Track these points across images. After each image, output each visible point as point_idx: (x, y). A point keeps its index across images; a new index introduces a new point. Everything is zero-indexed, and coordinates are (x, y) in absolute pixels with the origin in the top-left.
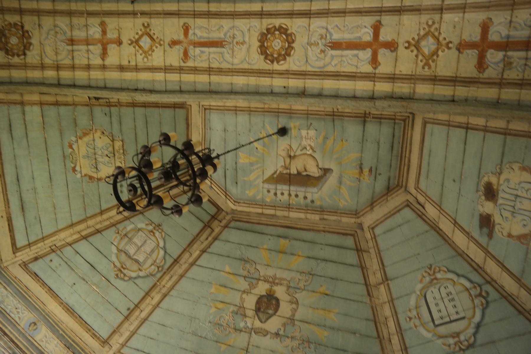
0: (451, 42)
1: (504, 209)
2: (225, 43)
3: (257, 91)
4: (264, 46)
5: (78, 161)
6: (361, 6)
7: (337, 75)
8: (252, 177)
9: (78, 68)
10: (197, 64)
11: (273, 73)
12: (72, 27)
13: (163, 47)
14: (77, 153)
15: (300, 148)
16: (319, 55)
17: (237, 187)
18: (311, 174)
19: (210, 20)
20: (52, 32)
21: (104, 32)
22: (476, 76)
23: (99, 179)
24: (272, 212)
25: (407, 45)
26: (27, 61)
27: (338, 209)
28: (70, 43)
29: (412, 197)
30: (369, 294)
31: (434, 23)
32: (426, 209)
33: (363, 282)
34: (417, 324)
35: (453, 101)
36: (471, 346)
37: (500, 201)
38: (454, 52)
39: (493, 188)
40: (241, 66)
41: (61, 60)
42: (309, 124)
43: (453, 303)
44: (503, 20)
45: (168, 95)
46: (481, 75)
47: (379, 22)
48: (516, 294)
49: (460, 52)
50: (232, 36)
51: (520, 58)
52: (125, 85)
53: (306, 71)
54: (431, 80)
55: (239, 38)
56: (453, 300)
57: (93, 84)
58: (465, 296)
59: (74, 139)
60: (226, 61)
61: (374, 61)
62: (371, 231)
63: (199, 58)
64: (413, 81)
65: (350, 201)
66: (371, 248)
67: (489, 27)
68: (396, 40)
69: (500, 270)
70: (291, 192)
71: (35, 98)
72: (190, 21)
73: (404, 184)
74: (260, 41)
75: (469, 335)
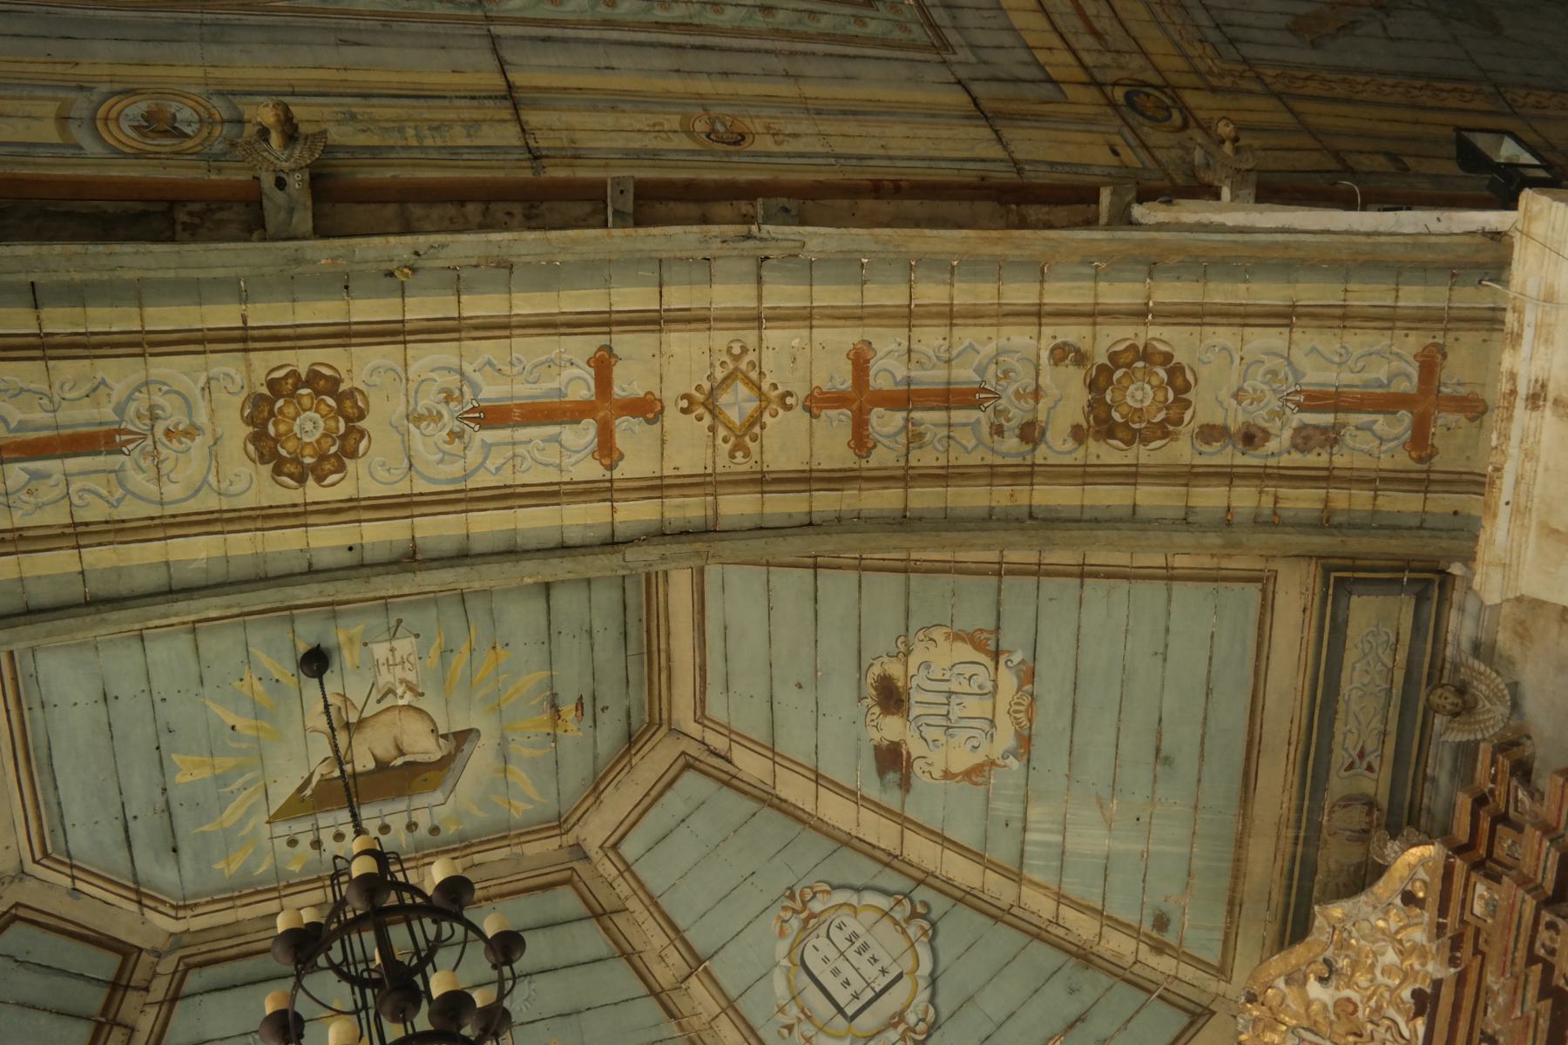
0: (789, 394)
1: (928, 725)
2: (124, 438)
6: (555, 310)
7: (505, 496)
8: (230, 816)
10: (19, 520)
11: (305, 513)
15: (375, 696)
16: (447, 447)
17: (178, 862)
18: (420, 758)
19: (51, 363)
22: (850, 465)
25: (685, 404)
29: (693, 742)
30: (671, 1015)
31: (744, 350)
32: (736, 762)
33: (644, 990)
34: (808, 1034)
35: (811, 524)
36: (933, 1027)
37: (916, 711)
38: (799, 418)
39: (897, 688)
40: (193, 505)
42: (393, 623)
43: (867, 955)
44: (893, 346)
46: (864, 464)
47: (608, 349)
48: (978, 885)
49: (813, 416)
50: (144, 411)
51: (935, 425)
54: (752, 481)
55: (173, 414)
56: (865, 947)
58: (885, 927)
60: (134, 494)
61: (606, 449)
62: (611, 854)
63: (25, 498)
64: (710, 490)
65: (535, 795)
66: (627, 899)
67: (868, 361)
68: (657, 394)
69: (939, 848)
73: (665, 716)
74: (250, 421)
75: (922, 1007)
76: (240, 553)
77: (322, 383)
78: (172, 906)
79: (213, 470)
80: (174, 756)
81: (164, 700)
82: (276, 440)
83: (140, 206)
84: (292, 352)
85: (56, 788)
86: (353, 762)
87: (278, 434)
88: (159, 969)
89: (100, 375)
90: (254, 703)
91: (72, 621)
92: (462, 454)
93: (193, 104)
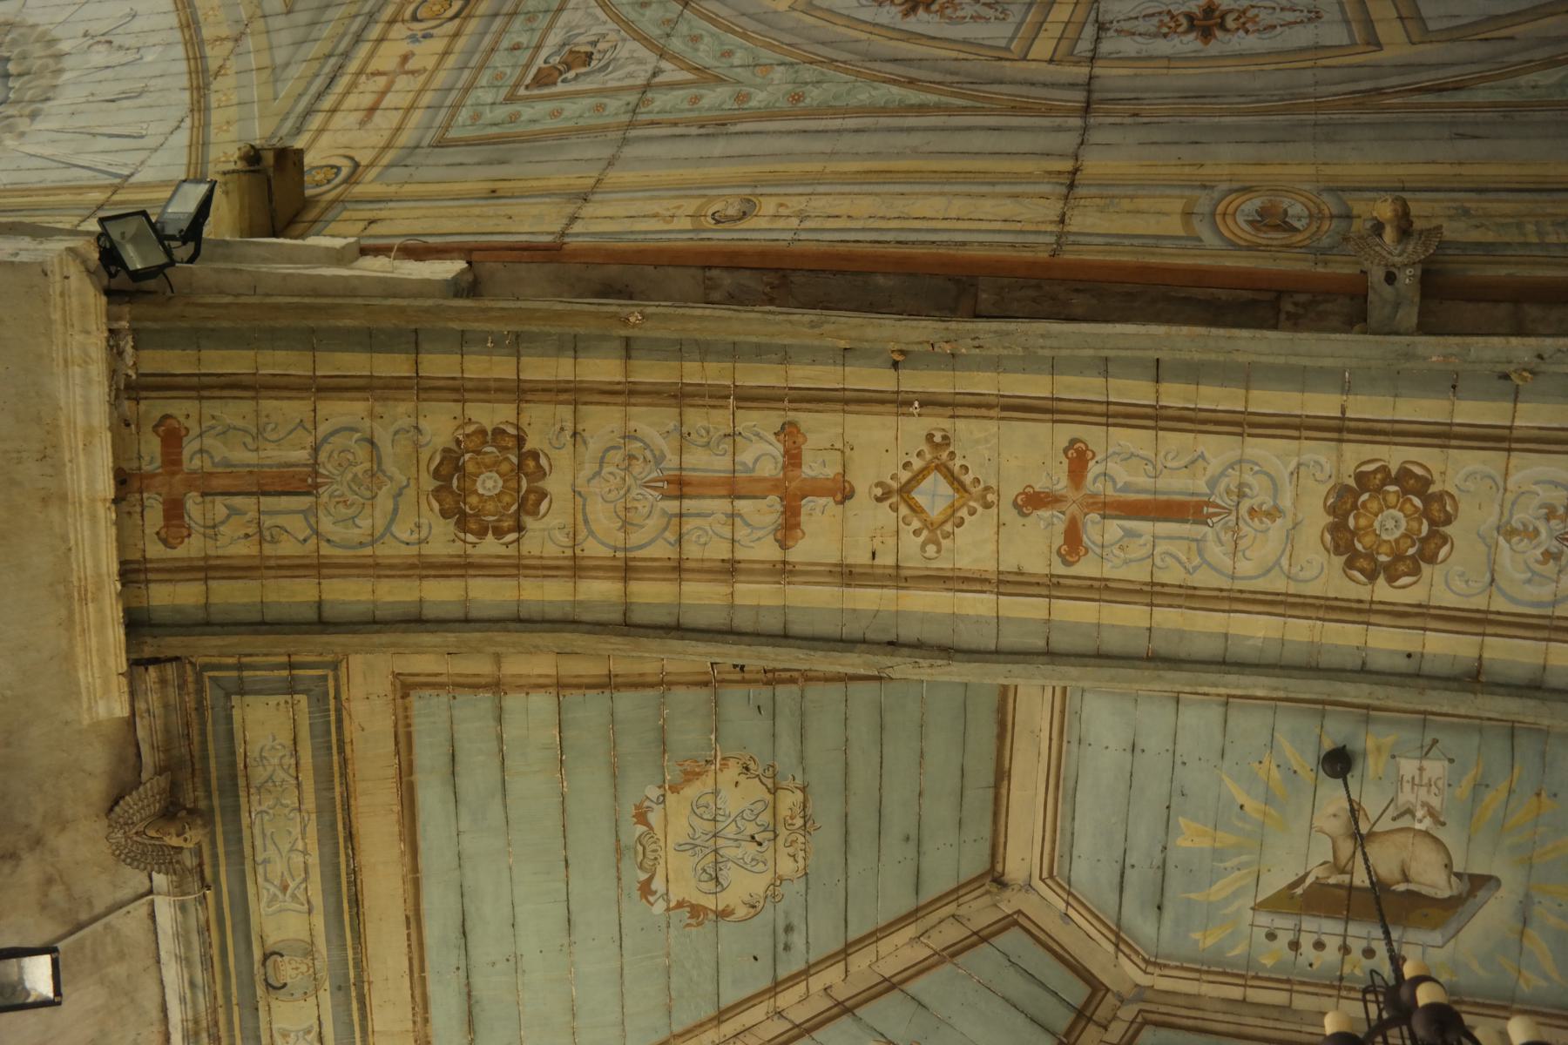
2: (1211, 510)
3: (1314, 664)
4: (1346, 526)
5: (662, 861)
8: (1219, 891)
9: (693, 571)
10: (1108, 571)
11: (1370, 611)
12: (683, 440)
13: (994, 510)
14: (660, 835)
15: (1391, 812)
16: (1538, 568)
17: (1159, 922)
18: (1424, 890)
19: (1161, 433)
20: (616, 456)
21: (793, 458)
23: (723, 914)
24: (1279, 998)
26: (524, 552)
27: (1513, 1000)
28: (674, 489)
40: (1261, 584)
41: (641, 547)
42: (1428, 741)
45: (1009, 666)
52: (854, 629)
53: (1488, 612)
55: (1260, 495)
57: (743, 622)
59: (653, 792)
60: (1209, 565)
63: (1116, 552)
70: (1349, 941)
71: (542, 666)
72: (1092, 435)
74: (1331, 510)
76: (1296, 638)
77: (1412, 482)
78: (1144, 960)
79: (1287, 553)
80: (1181, 820)
81: (1184, 763)
82: (1354, 533)
83: (1248, 295)
84: (1386, 447)
85: (1073, 819)
86: (1352, 874)
87: (1357, 528)
88: (1119, 1013)
89: (1200, 449)
90: (1267, 788)
91: (1132, 672)
92: (1555, 577)
93: (1303, 199)
